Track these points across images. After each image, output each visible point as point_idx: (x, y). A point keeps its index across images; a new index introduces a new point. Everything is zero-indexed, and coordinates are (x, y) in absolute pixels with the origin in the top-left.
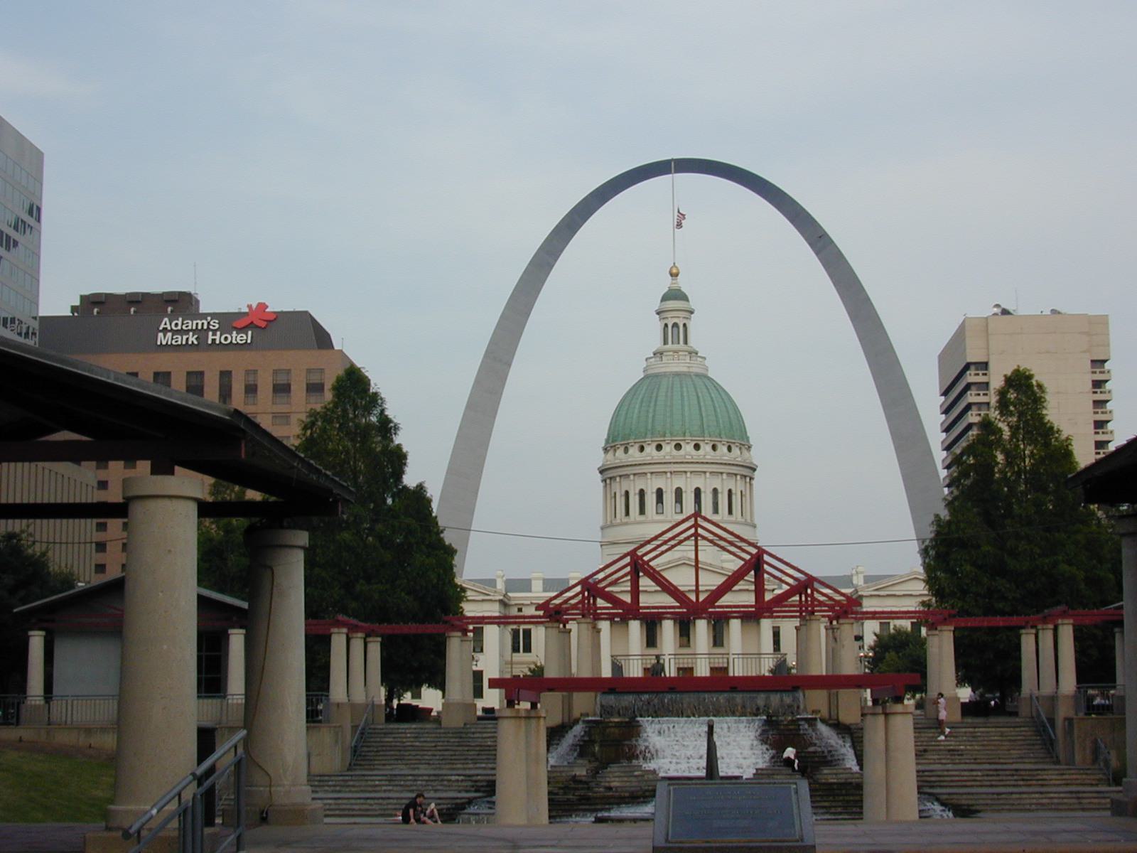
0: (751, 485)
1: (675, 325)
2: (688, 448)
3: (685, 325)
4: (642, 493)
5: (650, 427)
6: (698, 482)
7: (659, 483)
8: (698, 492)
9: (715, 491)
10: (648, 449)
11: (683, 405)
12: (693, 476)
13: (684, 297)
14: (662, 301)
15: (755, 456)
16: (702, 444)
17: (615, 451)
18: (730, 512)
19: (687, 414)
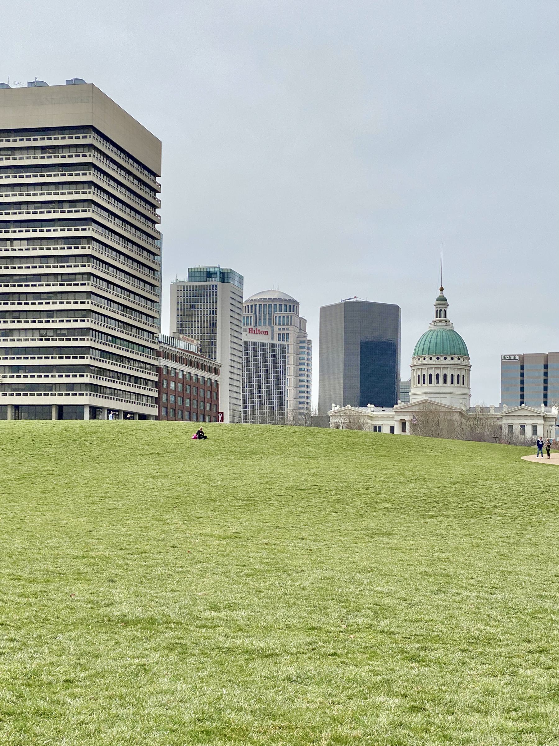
0: (469, 373)
1: (441, 310)
3: (445, 310)
6: (445, 372)
8: (445, 376)
10: (427, 359)
13: (445, 300)
15: (471, 362)
18: (458, 383)
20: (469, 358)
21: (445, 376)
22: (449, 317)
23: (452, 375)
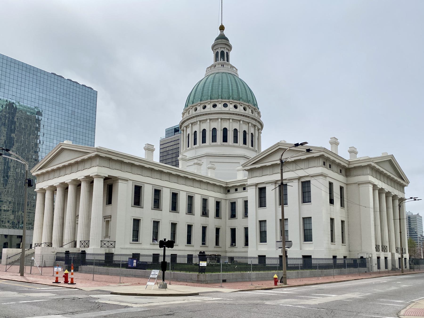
2: (231, 107)
4: (204, 131)
5: (210, 94)
6: (236, 126)
8: (236, 131)
16: (238, 105)
17: (189, 111)
21: (236, 131)
23: (245, 132)
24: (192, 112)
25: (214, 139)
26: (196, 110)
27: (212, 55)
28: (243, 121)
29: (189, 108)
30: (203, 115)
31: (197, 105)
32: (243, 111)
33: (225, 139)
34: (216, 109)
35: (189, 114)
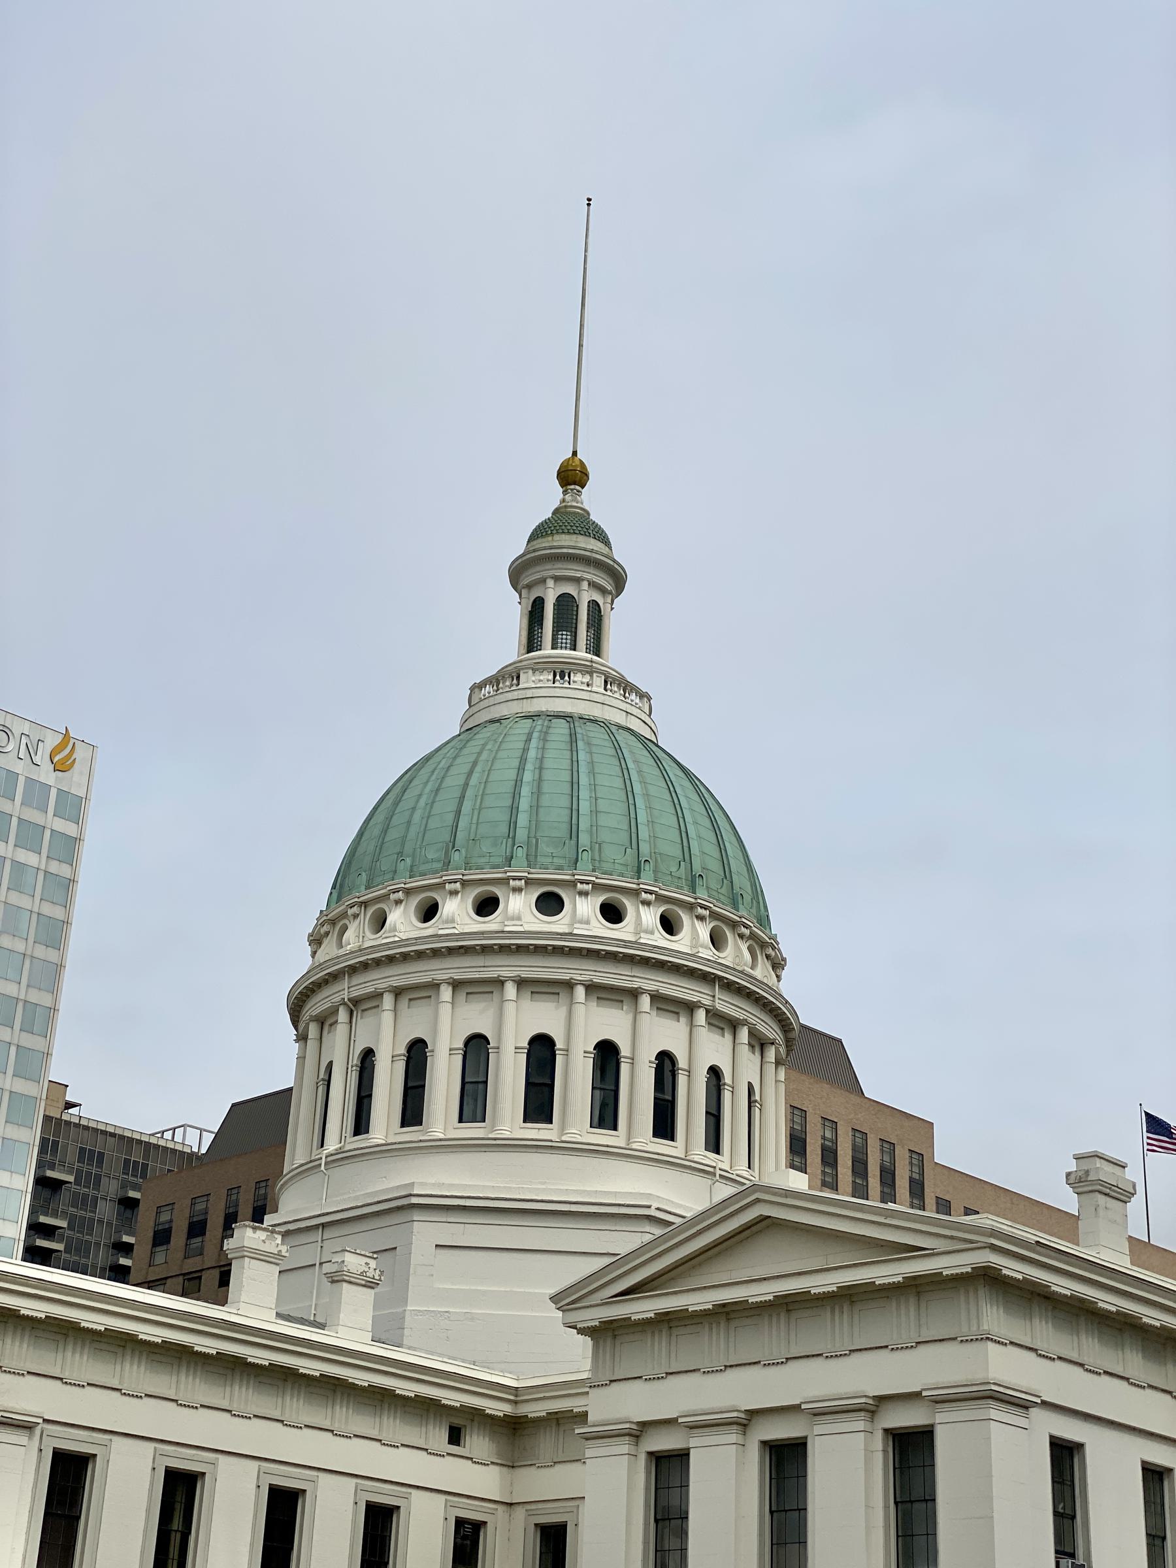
1: (566, 604)
2: (582, 916)
3: (594, 606)
7: (476, 1017)
9: (665, 1061)
11: (574, 784)
12: (593, 1004)
14: (529, 542)
17: (344, 929)
18: (714, 1144)
19: (585, 807)
20: (777, 965)
21: (607, 1053)
22: (618, 653)
24: (357, 937)
25: (473, 1101)
26: (380, 922)
27: (511, 612)
28: (656, 998)
29: (344, 915)
30: (420, 955)
31: (385, 897)
32: (660, 938)
33: (539, 1106)
34: (491, 923)
35: (340, 945)
